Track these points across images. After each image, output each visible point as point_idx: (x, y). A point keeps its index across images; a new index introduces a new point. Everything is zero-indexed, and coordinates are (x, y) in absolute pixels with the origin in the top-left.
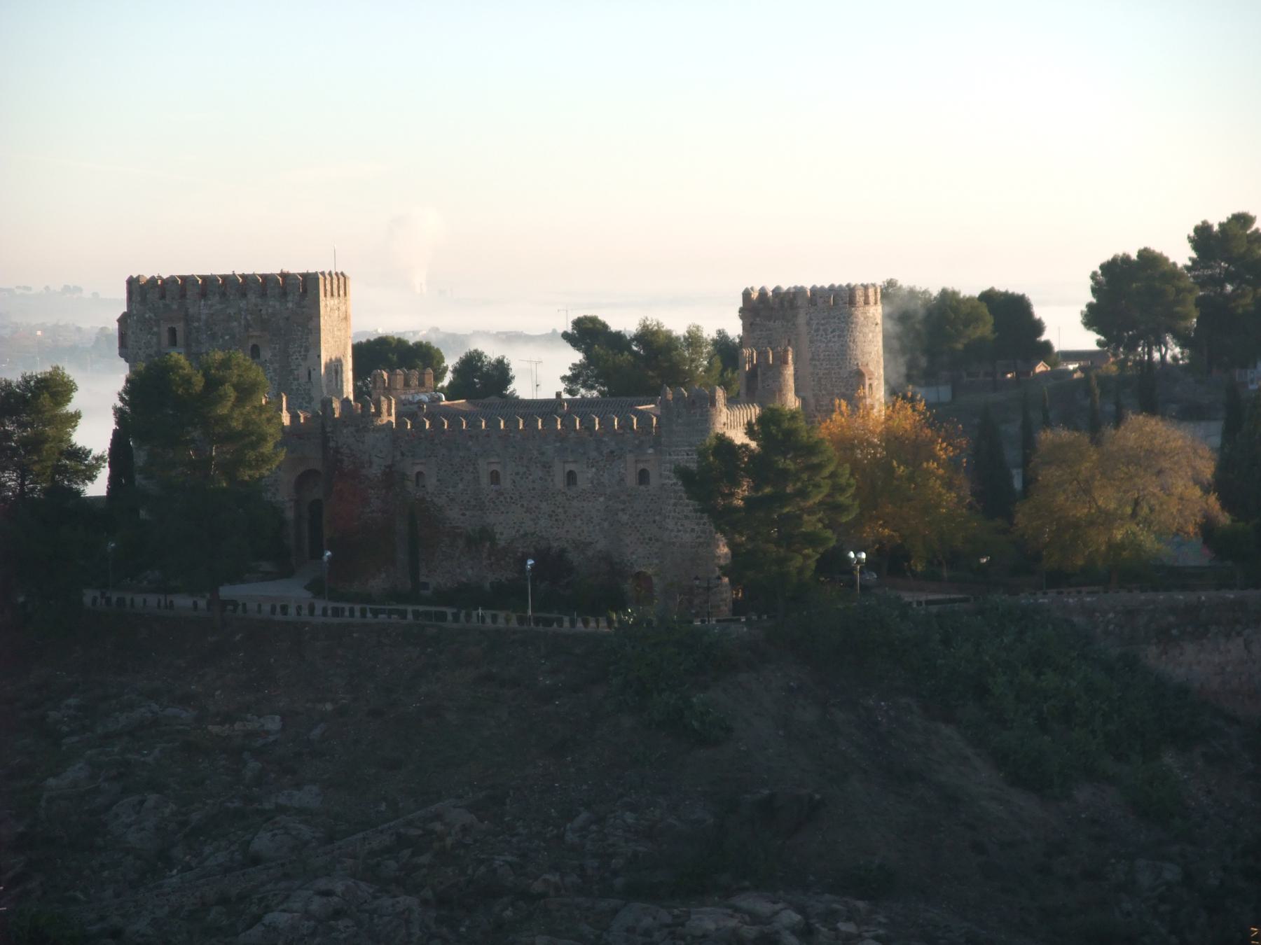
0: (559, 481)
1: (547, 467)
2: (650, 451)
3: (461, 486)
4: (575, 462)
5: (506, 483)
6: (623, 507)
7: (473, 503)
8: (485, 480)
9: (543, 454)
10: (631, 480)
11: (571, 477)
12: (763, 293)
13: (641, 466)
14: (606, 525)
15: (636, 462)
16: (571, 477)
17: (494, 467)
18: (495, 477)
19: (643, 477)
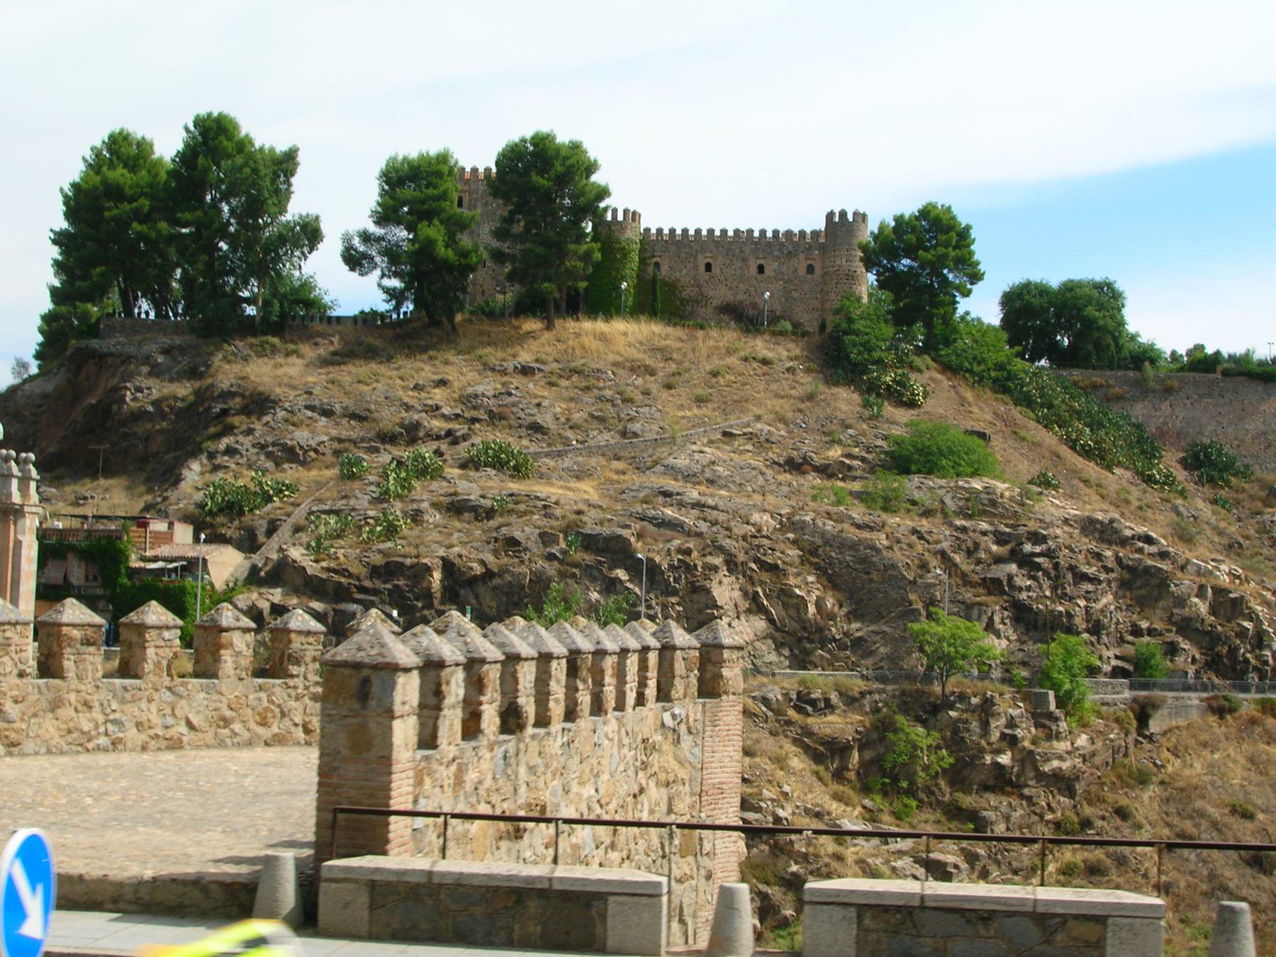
0: (753, 270)
1: (744, 260)
2: (816, 252)
3: (685, 271)
4: (765, 258)
5: (716, 270)
6: (794, 287)
7: (692, 282)
8: (702, 268)
9: (742, 252)
10: (802, 271)
11: (761, 269)
12: (776, 232)
13: (809, 262)
14: (783, 299)
15: (807, 259)
16: (761, 269)
17: (709, 260)
18: (708, 267)
19: (810, 269)
